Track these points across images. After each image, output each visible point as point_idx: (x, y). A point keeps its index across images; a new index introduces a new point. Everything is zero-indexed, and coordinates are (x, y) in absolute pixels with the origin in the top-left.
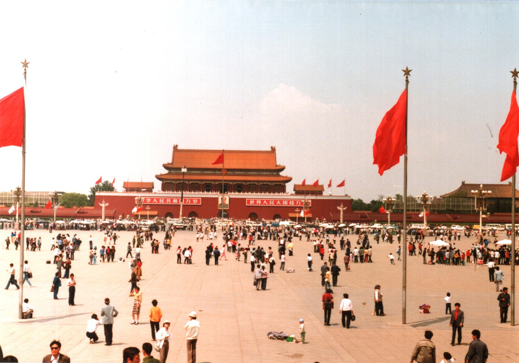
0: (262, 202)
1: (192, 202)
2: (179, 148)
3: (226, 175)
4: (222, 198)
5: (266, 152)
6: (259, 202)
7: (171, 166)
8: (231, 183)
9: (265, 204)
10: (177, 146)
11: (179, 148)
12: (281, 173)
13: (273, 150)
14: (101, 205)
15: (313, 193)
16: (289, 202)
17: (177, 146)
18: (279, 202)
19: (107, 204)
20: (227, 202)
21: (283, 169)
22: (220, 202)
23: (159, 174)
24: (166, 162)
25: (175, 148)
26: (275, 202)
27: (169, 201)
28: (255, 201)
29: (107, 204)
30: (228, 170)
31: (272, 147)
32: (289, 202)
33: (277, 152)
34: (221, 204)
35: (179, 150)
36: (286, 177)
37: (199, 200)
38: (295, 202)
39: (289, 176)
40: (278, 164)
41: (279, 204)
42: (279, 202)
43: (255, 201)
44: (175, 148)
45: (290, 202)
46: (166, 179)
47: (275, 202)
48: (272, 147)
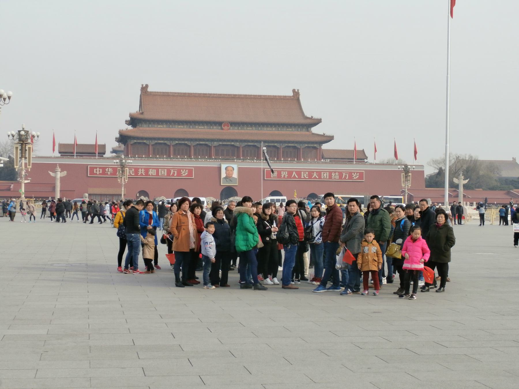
1: (179, 174)
2: (150, 89)
4: (226, 168)
8: (237, 144)
9: (295, 177)
10: (147, 86)
11: (150, 89)
12: (315, 130)
13: (296, 94)
14: (52, 174)
15: (350, 160)
16: (330, 173)
17: (147, 86)
18: (315, 174)
19: (65, 173)
20: (235, 175)
21: (318, 121)
22: (223, 175)
25: (144, 89)
27: (141, 172)
29: (65, 173)
30: (233, 124)
31: (294, 91)
33: (301, 98)
34: (226, 178)
35: (151, 92)
36: (324, 135)
38: (341, 174)
39: (328, 133)
40: (308, 114)
41: (315, 177)
42: (315, 174)
44: (144, 89)
45: (333, 174)
46: (134, 138)
47: (310, 174)
48: (294, 91)
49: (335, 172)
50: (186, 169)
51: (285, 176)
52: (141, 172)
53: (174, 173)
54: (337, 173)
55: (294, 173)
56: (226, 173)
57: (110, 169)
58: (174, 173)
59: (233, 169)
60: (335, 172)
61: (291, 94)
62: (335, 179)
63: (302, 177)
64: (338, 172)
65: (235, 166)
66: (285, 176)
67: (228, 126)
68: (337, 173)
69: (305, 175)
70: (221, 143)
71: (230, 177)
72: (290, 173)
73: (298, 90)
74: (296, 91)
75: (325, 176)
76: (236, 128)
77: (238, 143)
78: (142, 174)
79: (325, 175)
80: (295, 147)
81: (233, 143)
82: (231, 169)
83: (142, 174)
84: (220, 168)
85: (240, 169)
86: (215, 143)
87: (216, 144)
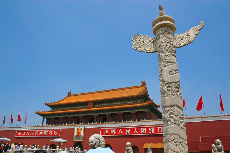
0: (117, 130)
3: (93, 107)
4: (77, 129)
5: (137, 87)
6: (113, 131)
7: (53, 104)
8: (94, 114)
9: (120, 133)
11: (71, 94)
16: (148, 128)
18: (136, 130)
20: (82, 134)
22: (75, 134)
23: (40, 111)
24: (49, 102)
26: (132, 130)
27: (37, 133)
28: (110, 130)
31: (142, 82)
32: (148, 128)
37: (59, 131)
42: (136, 130)
43: (110, 130)
45: (150, 129)
48: (142, 82)
49: (151, 127)
50: (57, 131)
51: (113, 133)
52: (37, 133)
53: (51, 133)
54: (153, 128)
55: (120, 130)
56: (77, 132)
57: (24, 132)
58: (51, 133)
59: (81, 129)
60: (151, 127)
61: (141, 84)
62: (151, 133)
63: (126, 133)
64: (154, 127)
65: (83, 128)
66: (113, 133)
67: (92, 105)
68: (153, 128)
69: (128, 131)
70: (85, 115)
71: (79, 135)
72: (117, 130)
73: (145, 81)
74: (144, 82)
75: (144, 131)
76: (98, 105)
77: (94, 114)
78: (36, 135)
79: (144, 130)
80: (130, 113)
81: (91, 114)
82: (80, 129)
83: (36, 135)
84: (74, 129)
85: (85, 129)
86: (82, 115)
87: (82, 115)
